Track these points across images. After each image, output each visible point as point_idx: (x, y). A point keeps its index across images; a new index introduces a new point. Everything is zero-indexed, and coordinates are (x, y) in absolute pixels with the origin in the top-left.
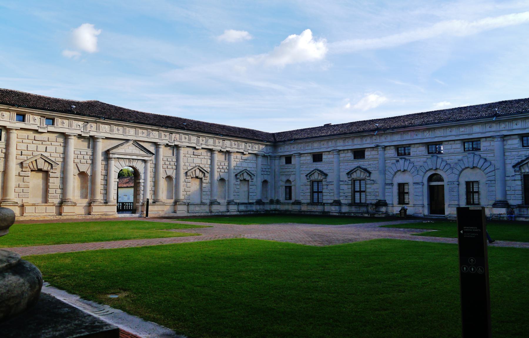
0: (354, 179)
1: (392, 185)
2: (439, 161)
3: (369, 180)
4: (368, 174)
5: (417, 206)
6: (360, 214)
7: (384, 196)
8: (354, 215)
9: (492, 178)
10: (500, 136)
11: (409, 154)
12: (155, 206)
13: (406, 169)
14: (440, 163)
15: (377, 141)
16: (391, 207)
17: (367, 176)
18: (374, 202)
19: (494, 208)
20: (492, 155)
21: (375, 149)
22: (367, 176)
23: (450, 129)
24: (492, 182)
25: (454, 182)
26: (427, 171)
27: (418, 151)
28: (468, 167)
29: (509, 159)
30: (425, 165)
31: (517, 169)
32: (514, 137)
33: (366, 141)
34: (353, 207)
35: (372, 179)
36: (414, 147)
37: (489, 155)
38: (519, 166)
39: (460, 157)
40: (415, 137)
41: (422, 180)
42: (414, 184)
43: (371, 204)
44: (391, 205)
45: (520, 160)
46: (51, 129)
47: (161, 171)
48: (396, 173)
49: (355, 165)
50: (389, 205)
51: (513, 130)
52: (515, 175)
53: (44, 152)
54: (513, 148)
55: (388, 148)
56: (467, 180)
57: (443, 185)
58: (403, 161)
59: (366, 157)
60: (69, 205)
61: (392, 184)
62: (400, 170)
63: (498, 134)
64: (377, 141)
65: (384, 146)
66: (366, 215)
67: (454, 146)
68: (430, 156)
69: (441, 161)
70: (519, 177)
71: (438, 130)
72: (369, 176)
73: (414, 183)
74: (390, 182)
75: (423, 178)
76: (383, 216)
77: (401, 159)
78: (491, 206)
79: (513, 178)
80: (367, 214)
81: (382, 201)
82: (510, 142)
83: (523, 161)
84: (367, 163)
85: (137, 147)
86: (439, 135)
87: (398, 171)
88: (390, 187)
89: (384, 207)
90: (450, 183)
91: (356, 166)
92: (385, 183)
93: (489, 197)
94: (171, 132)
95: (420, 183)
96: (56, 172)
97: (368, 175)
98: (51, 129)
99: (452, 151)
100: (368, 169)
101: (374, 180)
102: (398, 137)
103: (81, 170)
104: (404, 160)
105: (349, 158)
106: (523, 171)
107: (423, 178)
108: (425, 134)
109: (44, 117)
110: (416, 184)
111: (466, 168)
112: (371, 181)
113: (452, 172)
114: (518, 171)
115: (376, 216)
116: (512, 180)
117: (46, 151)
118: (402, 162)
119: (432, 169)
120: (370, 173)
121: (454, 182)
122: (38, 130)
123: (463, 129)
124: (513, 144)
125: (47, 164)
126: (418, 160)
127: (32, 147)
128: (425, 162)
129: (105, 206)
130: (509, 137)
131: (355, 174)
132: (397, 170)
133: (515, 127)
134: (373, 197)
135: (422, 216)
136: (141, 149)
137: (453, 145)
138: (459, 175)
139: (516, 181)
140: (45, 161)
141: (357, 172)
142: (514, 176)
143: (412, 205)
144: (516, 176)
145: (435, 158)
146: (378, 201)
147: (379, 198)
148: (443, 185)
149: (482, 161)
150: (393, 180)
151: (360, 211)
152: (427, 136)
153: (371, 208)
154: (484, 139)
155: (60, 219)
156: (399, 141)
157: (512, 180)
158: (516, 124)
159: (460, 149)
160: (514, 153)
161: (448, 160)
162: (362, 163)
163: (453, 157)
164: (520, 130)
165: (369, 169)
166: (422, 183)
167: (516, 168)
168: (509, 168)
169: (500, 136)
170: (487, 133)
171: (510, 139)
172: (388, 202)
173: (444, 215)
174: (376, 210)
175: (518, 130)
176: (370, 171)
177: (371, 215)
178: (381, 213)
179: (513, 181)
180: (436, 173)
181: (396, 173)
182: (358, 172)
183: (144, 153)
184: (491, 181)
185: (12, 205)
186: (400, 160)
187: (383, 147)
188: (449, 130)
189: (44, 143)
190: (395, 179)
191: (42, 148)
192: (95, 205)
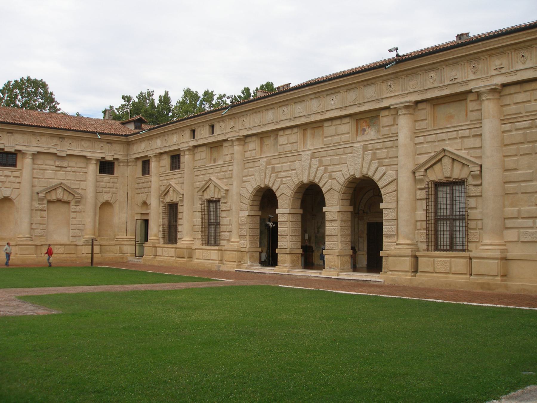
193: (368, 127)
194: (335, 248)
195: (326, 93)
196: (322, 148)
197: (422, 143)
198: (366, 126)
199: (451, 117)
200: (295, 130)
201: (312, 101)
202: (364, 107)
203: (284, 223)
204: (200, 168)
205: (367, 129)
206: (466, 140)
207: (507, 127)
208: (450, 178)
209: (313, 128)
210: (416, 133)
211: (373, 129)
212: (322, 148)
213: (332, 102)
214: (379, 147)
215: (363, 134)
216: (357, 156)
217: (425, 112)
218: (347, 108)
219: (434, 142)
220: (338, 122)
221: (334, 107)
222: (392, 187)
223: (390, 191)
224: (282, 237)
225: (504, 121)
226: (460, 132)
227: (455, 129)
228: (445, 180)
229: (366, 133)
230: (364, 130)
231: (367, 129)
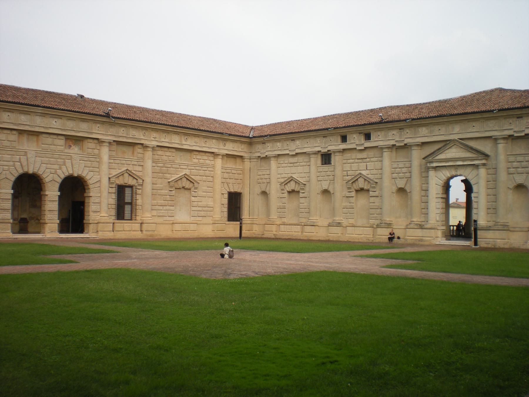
12: (491, 231)
46: (368, 144)
47: (503, 176)
53: (365, 170)
60: (382, 226)
85: (463, 148)
94: (518, 116)
96: (375, 190)
98: (368, 144)
103: (399, 187)
109: (362, 133)
117: (367, 169)
122: (356, 148)
125: (366, 183)
127: (355, 166)
129: (420, 230)
136: (467, 150)
140: (365, 179)
155: (372, 242)
183: (472, 154)
185: (335, 225)
189: (365, 160)
191: (363, 165)
192: (409, 227)
193: (73, 145)
194: (55, 219)
195: (51, 116)
196: (40, 151)
197: (112, 163)
198: (72, 144)
199: (124, 153)
200: (15, 132)
201: (37, 117)
202: (79, 134)
203: (6, 200)
204: (59, 152)
205: (72, 146)
206: (134, 166)
207: (112, 161)
208: (126, 184)
209: (28, 134)
210: (110, 157)
211: (77, 147)
212: (40, 151)
213: (55, 123)
214: (85, 160)
215: (70, 148)
216: (75, 163)
217: (114, 147)
218: (80, 132)
219: (119, 164)
220: (55, 137)
221: (55, 127)
222: (98, 185)
223: (96, 187)
224: (4, 211)
225: (153, 162)
226: (132, 162)
227: (130, 160)
228: (124, 184)
229: (71, 148)
230: (70, 146)
231: (72, 146)
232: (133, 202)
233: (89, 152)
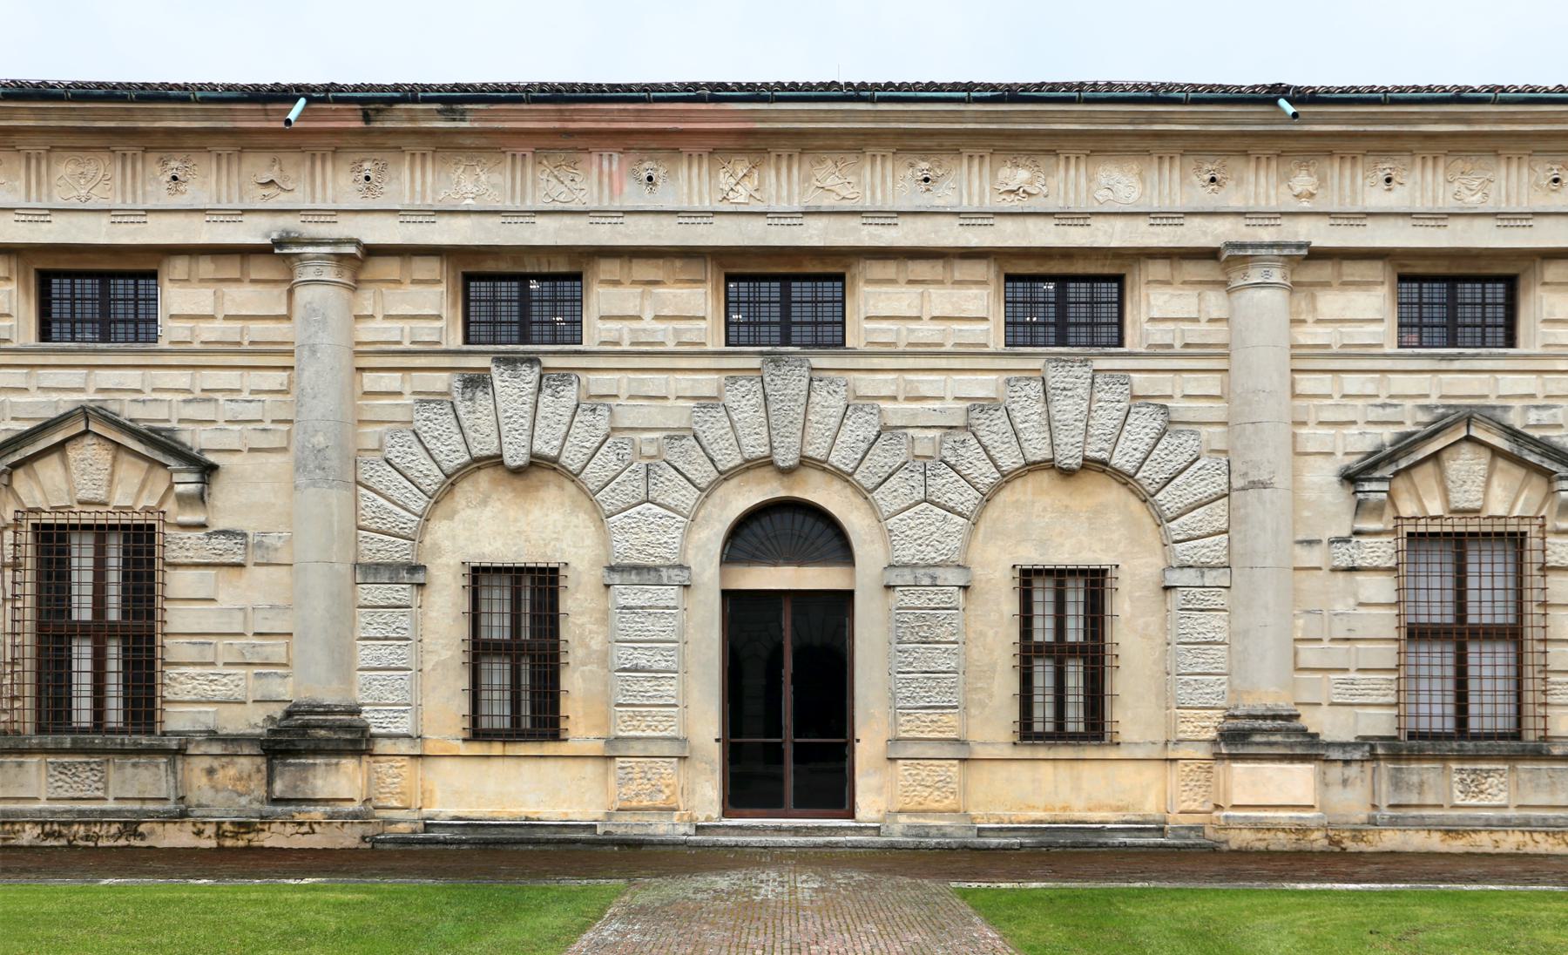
0: (47, 519)
1: (419, 578)
2: (828, 403)
3: (201, 533)
4: (194, 477)
5: (638, 749)
6: (114, 829)
7: (343, 665)
8: (50, 842)
9: (1208, 551)
10: (1286, 252)
11: (572, 332)
13: (544, 448)
14: (834, 422)
15: (284, 197)
16: (406, 762)
17: (183, 499)
18: (251, 720)
19: (1238, 767)
20: (1212, 385)
21: (261, 269)
22: (183, 499)
23: (924, 165)
24: (1210, 578)
25: (936, 565)
26: (725, 476)
27: (648, 314)
28: (1048, 465)
29: (1321, 423)
30: (714, 429)
31: (1374, 489)
32: (1353, 270)
33: (173, 192)
34: (32, 761)
35: (221, 523)
36: (616, 283)
37: (1195, 385)
38: (1387, 471)
39: (983, 385)
40: (633, 195)
41: (683, 550)
42: (616, 578)
43: (212, 736)
44: (404, 747)
45: (1387, 435)
48: (453, 479)
49: (55, 397)
50: (382, 746)
51: (1369, 222)
52: (1357, 533)
54: (1344, 346)
55: (389, 268)
56: (1033, 557)
57: (843, 600)
58: (530, 388)
59: (170, 331)
61: (413, 572)
62: (496, 461)
63: (1266, 235)
64: (282, 201)
65: (357, 243)
66: (178, 837)
67: (942, 299)
68: (756, 362)
69: (838, 403)
70: (1380, 551)
71: (829, 163)
72: (201, 499)
73: (611, 569)
74: (397, 551)
75: (687, 532)
76: (348, 837)
77: (508, 361)
78: (1203, 752)
79: (1343, 556)
80: (189, 827)
81: (329, 711)
82: (1332, 303)
83: (1407, 444)
84: (181, 379)
86: (828, 202)
87: (479, 464)
88: (403, 593)
89: (348, 764)
90: (908, 577)
91: (67, 402)
92: (356, 565)
93: (1187, 683)
95: (664, 573)
97: (187, 483)
99: (926, 332)
100: (185, 438)
101: (245, 535)
102: (483, 178)
104: (530, 375)
105: (426, 332)
106: (1408, 508)
107: (687, 532)
108: (724, 180)
110: (634, 577)
111: (1032, 467)
112: (220, 543)
113: (922, 496)
114: (1378, 510)
115: (274, 838)
116: (1335, 570)
118: (512, 388)
119: (767, 463)
120: (207, 471)
121: (939, 572)
123: (1022, 175)
124: (1348, 316)
126: (655, 383)
128: (707, 403)
130: (1325, 271)
131: (50, 470)
132: (467, 457)
133: (1377, 198)
134: (240, 682)
135: (682, 829)
137: (934, 292)
138: (974, 520)
139: (1360, 577)
141: (73, 453)
142: (1347, 540)
143: (597, 748)
144: (1363, 540)
145: (790, 381)
146: (278, 711)
147: (288, 690)
148: (848, 596)
149: (1143, 426)
150: (428, 540)
151: (110, 805)
152: (741, 197)
153: (211, 772)
154: (1158, 269)
156: (498, 219)
157: (1335, 570)
158: (1388, 180)
159: (983, 326)
160: (1353, 383)
161: (894, 398)
162: (132, 378)
163: (927, 383)
164: (1409, 222)
165: (196, 438)
166: (681, 567)
167: (1367, 486)
168: (1322, 478)
169: (1286, 252)
170: (906, 224)
171: (1326, 285)
172: (374, 720)
173: (852, 816)
174: (270, 782)
175: (1400, 222)
176: (212, 458)
177: (220, 835)
178: (317, 813)
179: (1340, 576)
180: (798, 494)
181: (453, 479)
182: (90, 457)
184: (1203, 568)
186: (500, 377)
187: (351, 250)
188: (912, 166)
190: (440, 530)
232: (1528, 620)
233: (1551, 340)
